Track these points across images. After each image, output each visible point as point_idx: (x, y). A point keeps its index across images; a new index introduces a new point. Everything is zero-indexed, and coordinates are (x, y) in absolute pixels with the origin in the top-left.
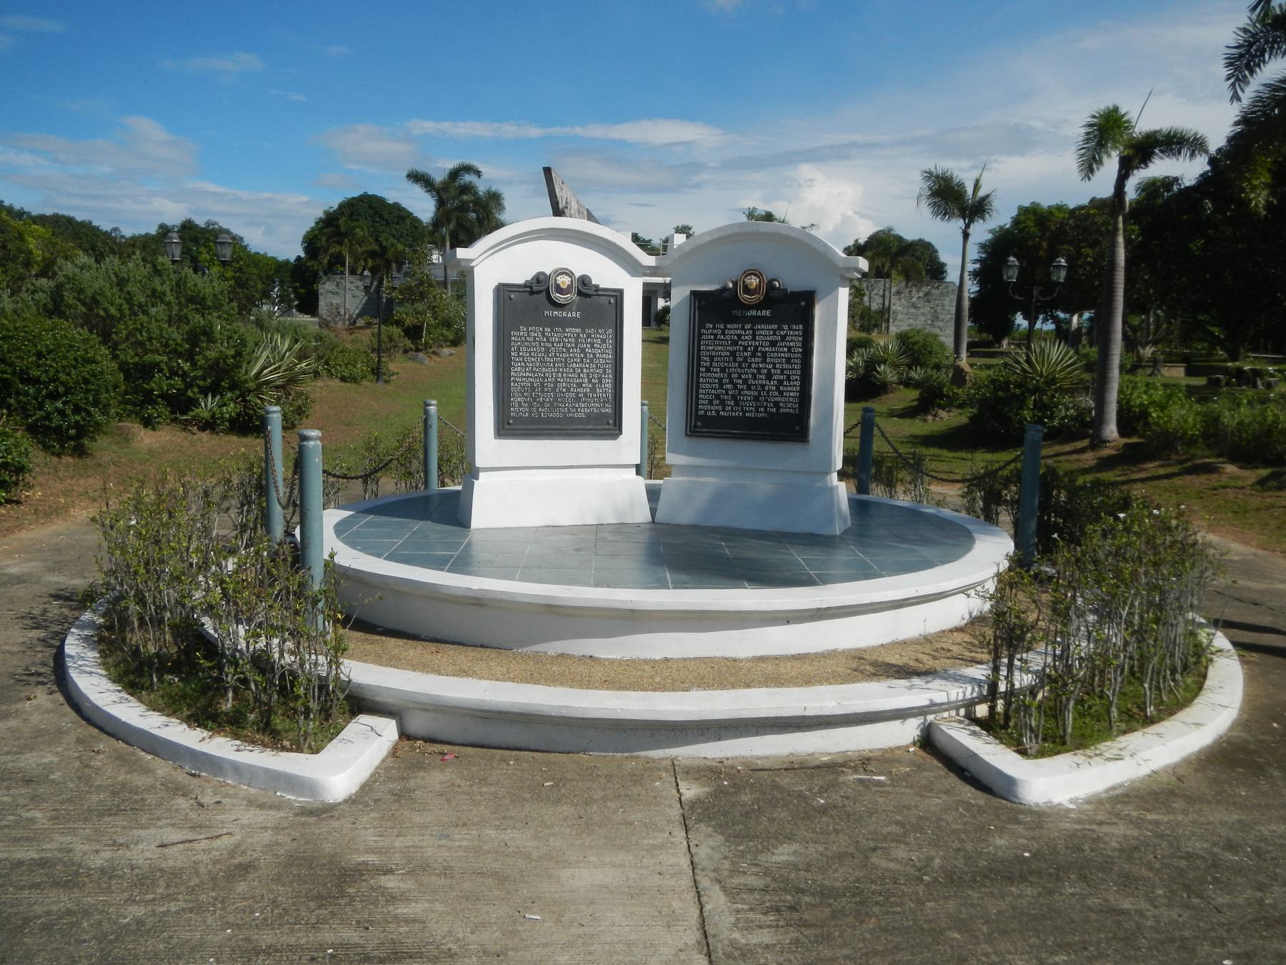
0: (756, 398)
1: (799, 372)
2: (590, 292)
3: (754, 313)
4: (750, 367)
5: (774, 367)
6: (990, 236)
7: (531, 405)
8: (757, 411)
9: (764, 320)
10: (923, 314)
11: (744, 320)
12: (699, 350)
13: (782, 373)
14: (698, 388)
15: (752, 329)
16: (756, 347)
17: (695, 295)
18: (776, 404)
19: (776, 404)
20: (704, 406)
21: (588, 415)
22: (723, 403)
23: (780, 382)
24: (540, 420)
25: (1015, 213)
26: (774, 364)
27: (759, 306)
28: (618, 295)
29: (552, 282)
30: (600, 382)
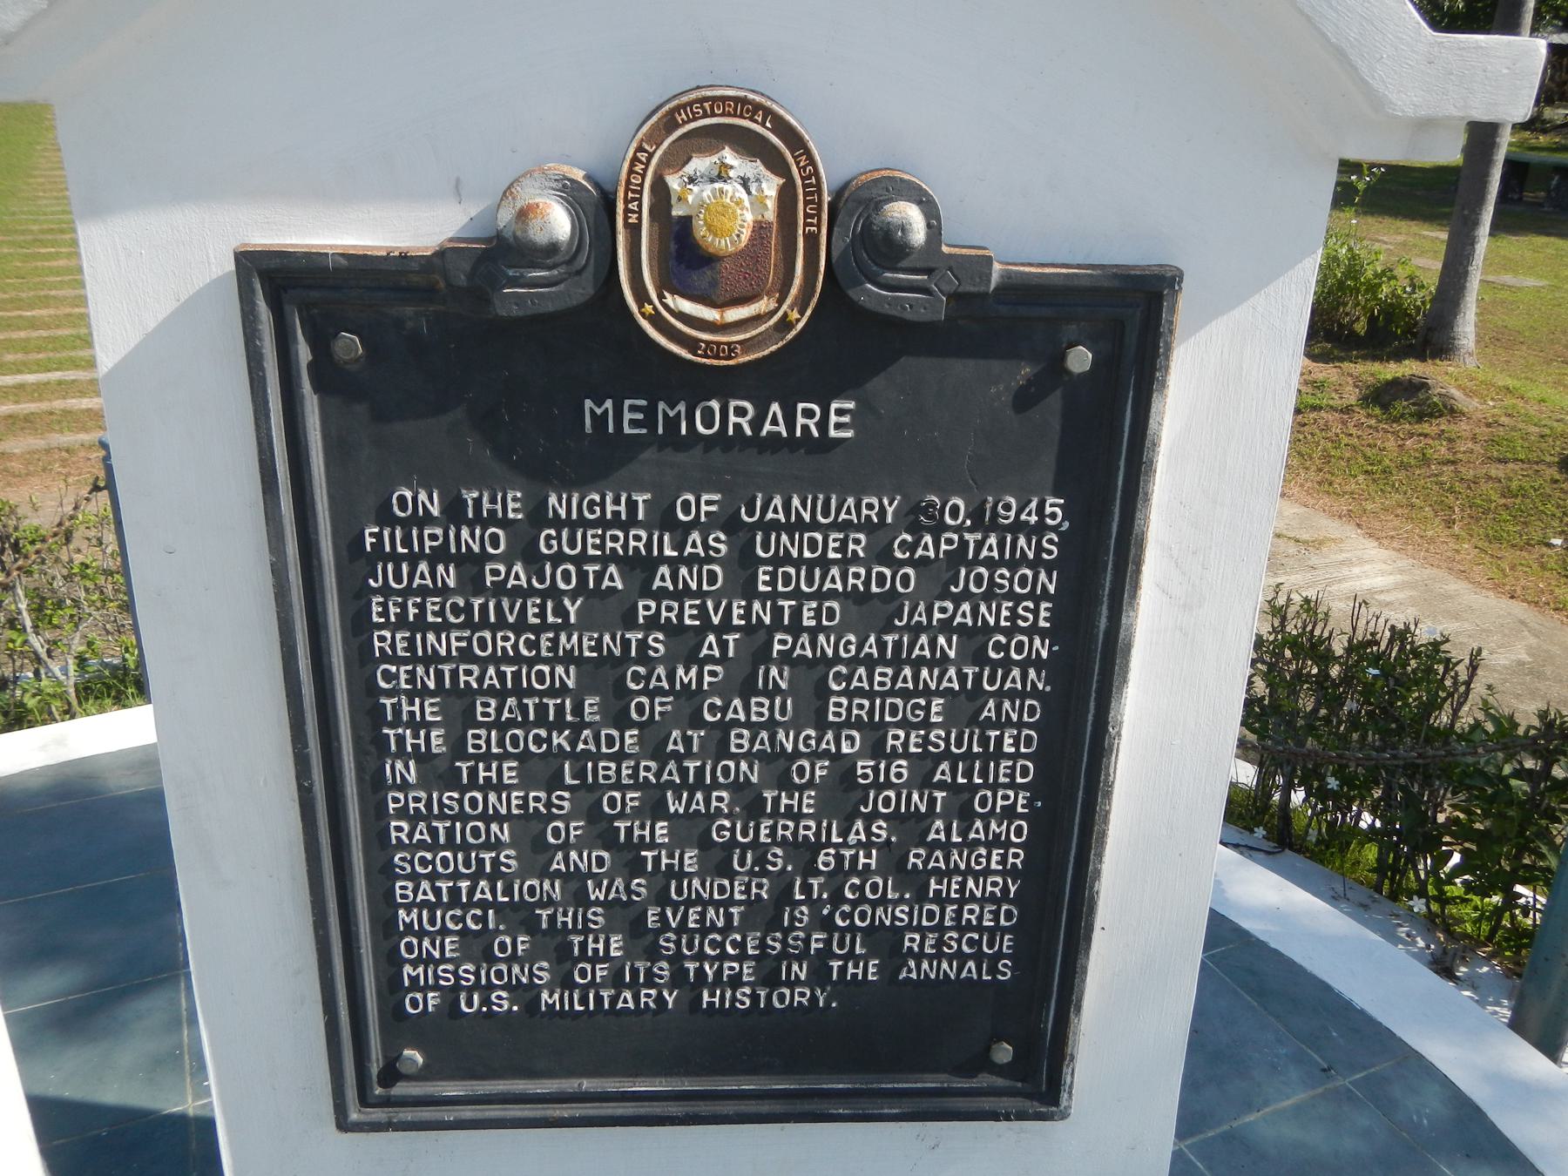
0: (766, 915)
3: (739, 416)
5: (876, 749)
8: (770, 979)
12: (362, 658)
13: (924, 781)
14: (383, 874)
17: (280, 284)
18: (886, 942)
20: (435, 970)
23: (911, 825)
26: (874, 734)
27: (777, 378)
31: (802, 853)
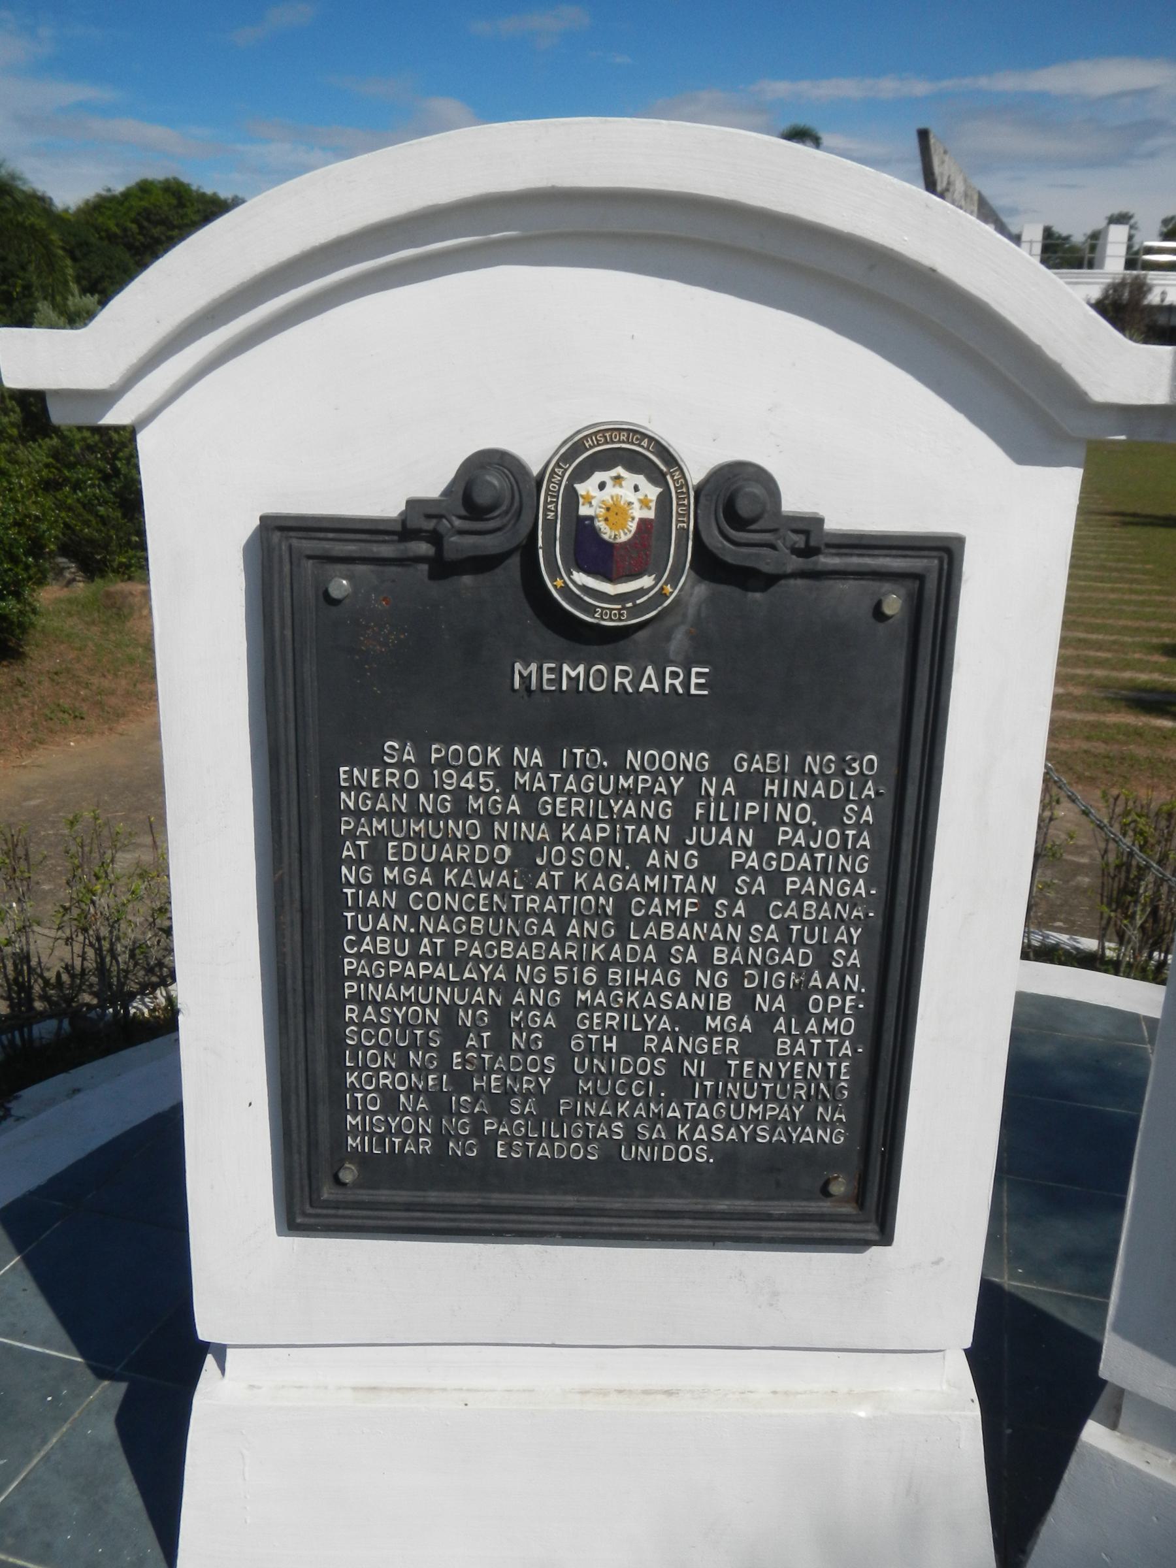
2: (767, 562)
7: (439, 1106)
21: (727, 1156)
24: (486, 1172)
28: (928, 573)
29: (549, 508)
30: (798, 1005)
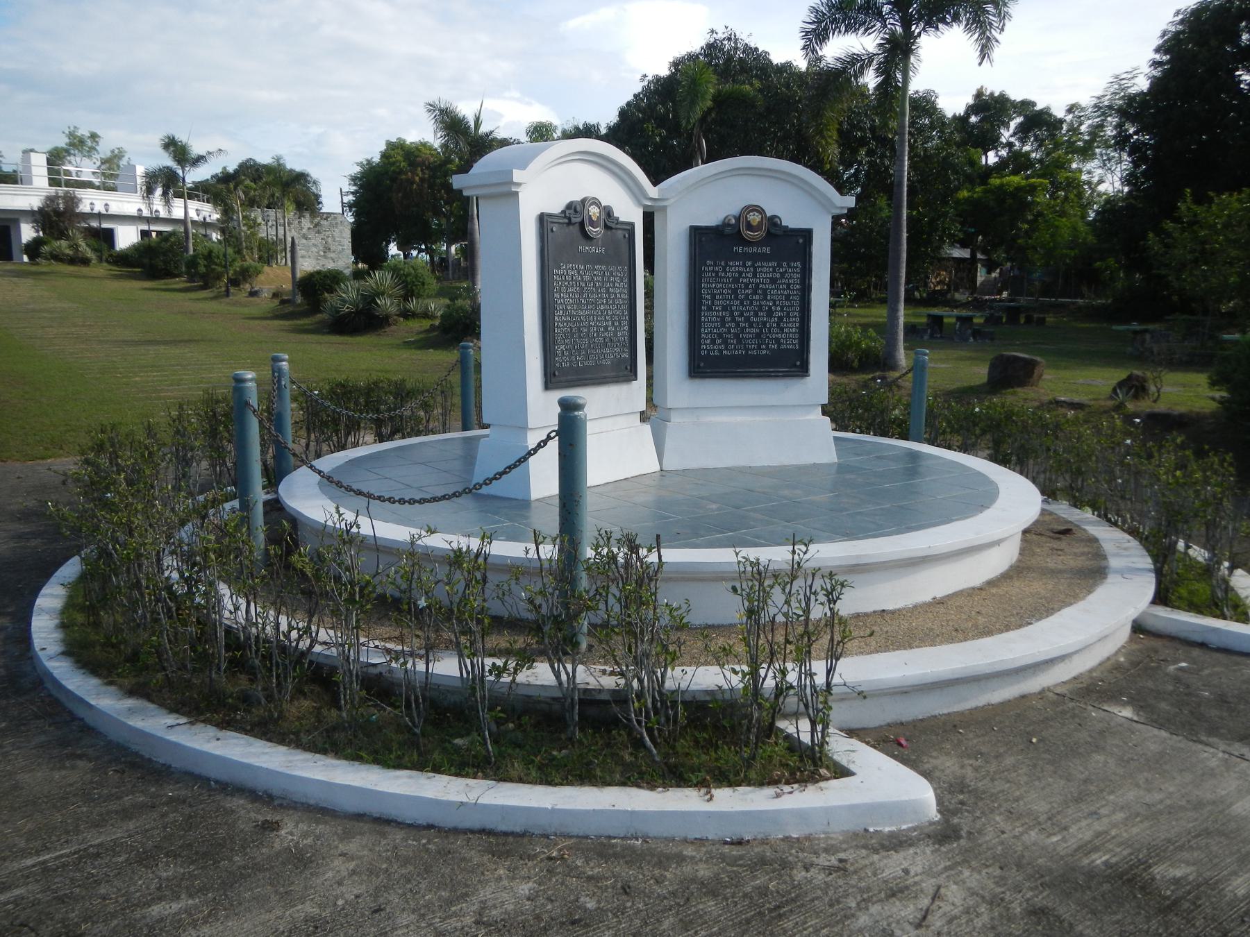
0: (758, 336)
1: (798, 309)
4: (751, 304)
5: (775, 304)
6: (358, 169)
9: (764, 257)
10: (315, 245)
11: (747, 257)
13: (782, 310)
15: (753, 266)
16: (757, 285)
19: (777, 341)
20: (706, 347)
22: (726, 342)
23: (781, 319)
25: (383, 147)
26: (775, 301)
31: (764, 323)
